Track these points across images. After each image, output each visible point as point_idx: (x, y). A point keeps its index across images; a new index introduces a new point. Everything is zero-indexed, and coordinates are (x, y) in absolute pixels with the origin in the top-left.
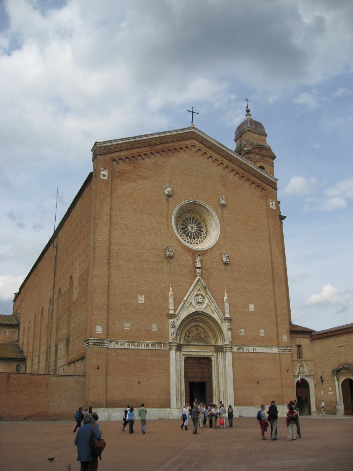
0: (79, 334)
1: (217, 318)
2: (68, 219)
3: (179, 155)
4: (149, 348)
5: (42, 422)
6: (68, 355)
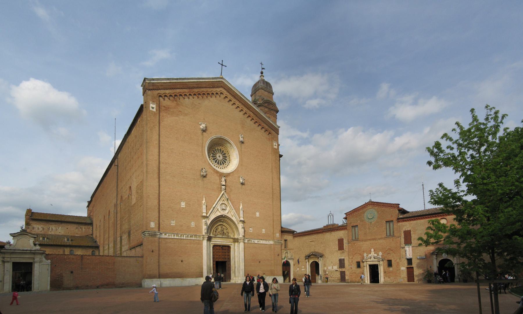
0: (138, 228)
2: (125, 144)
4: (189, 238)
5: (111, 290)
6: (130, 242)
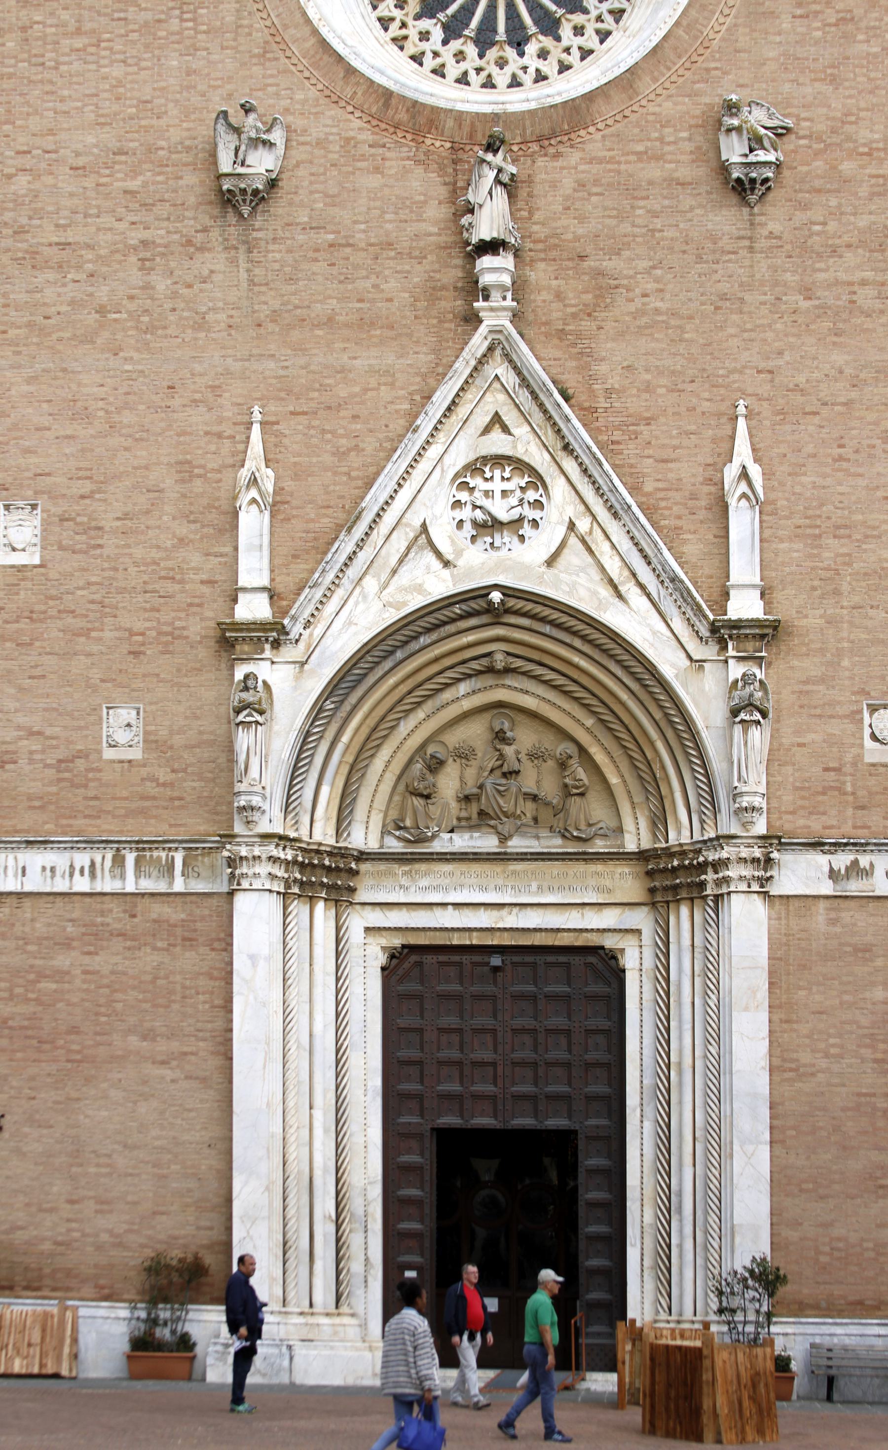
1: (655, 633)
4: (82, 884)
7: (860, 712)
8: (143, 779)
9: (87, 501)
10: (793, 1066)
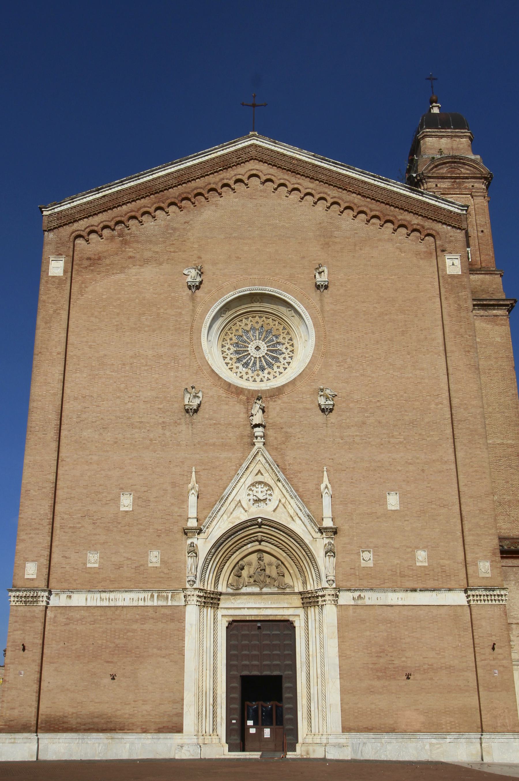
3: (221, 201)
4: (141, 603)
7: (360, 552)
8: (160, 572)
9: (146, 493)
10: (345, 655)
